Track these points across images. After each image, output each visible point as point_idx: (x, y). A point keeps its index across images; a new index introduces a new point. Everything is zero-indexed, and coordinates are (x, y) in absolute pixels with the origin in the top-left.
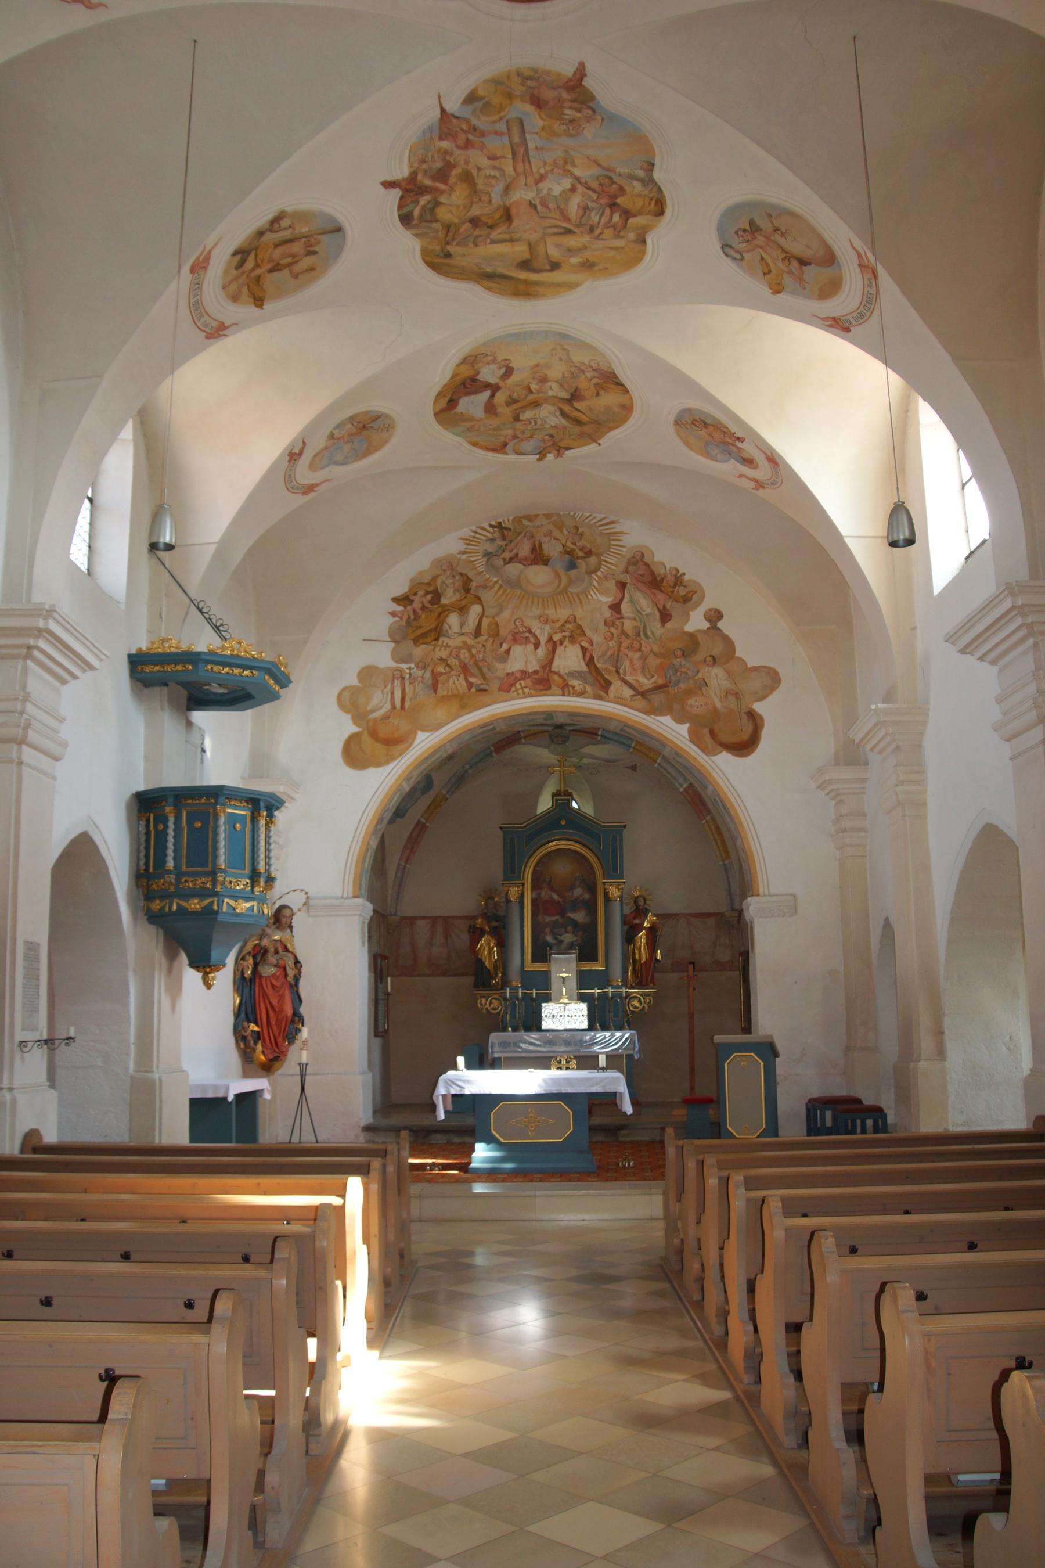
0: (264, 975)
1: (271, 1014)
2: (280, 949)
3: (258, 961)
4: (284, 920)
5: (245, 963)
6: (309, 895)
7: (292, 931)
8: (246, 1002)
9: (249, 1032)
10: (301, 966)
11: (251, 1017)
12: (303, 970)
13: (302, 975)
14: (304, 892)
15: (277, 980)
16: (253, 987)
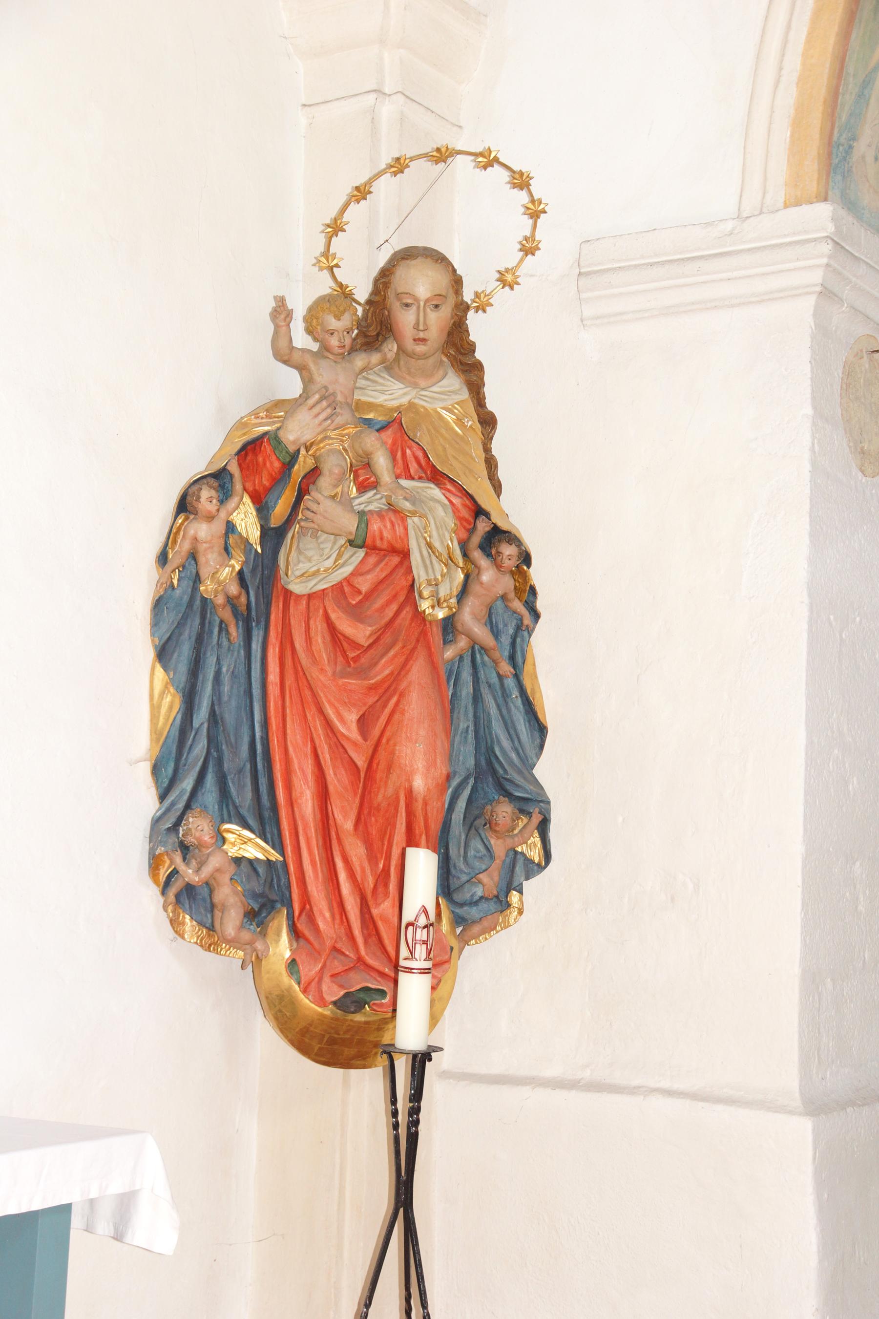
0: (297, 588)
1: (337, 779)
2: (382, 462)
3: (275, 521)
4: (405, 320)
5: (202, 530)
6: (536, 188)
7: (476, 389)
8: (214, 718)
9: (215, 862)
10: (526, 558)
11: (244, 797)
12: (537, 574)
13: (541, 604)
14: (522, 197)
15: (356, 613)
16: (256, 646)
